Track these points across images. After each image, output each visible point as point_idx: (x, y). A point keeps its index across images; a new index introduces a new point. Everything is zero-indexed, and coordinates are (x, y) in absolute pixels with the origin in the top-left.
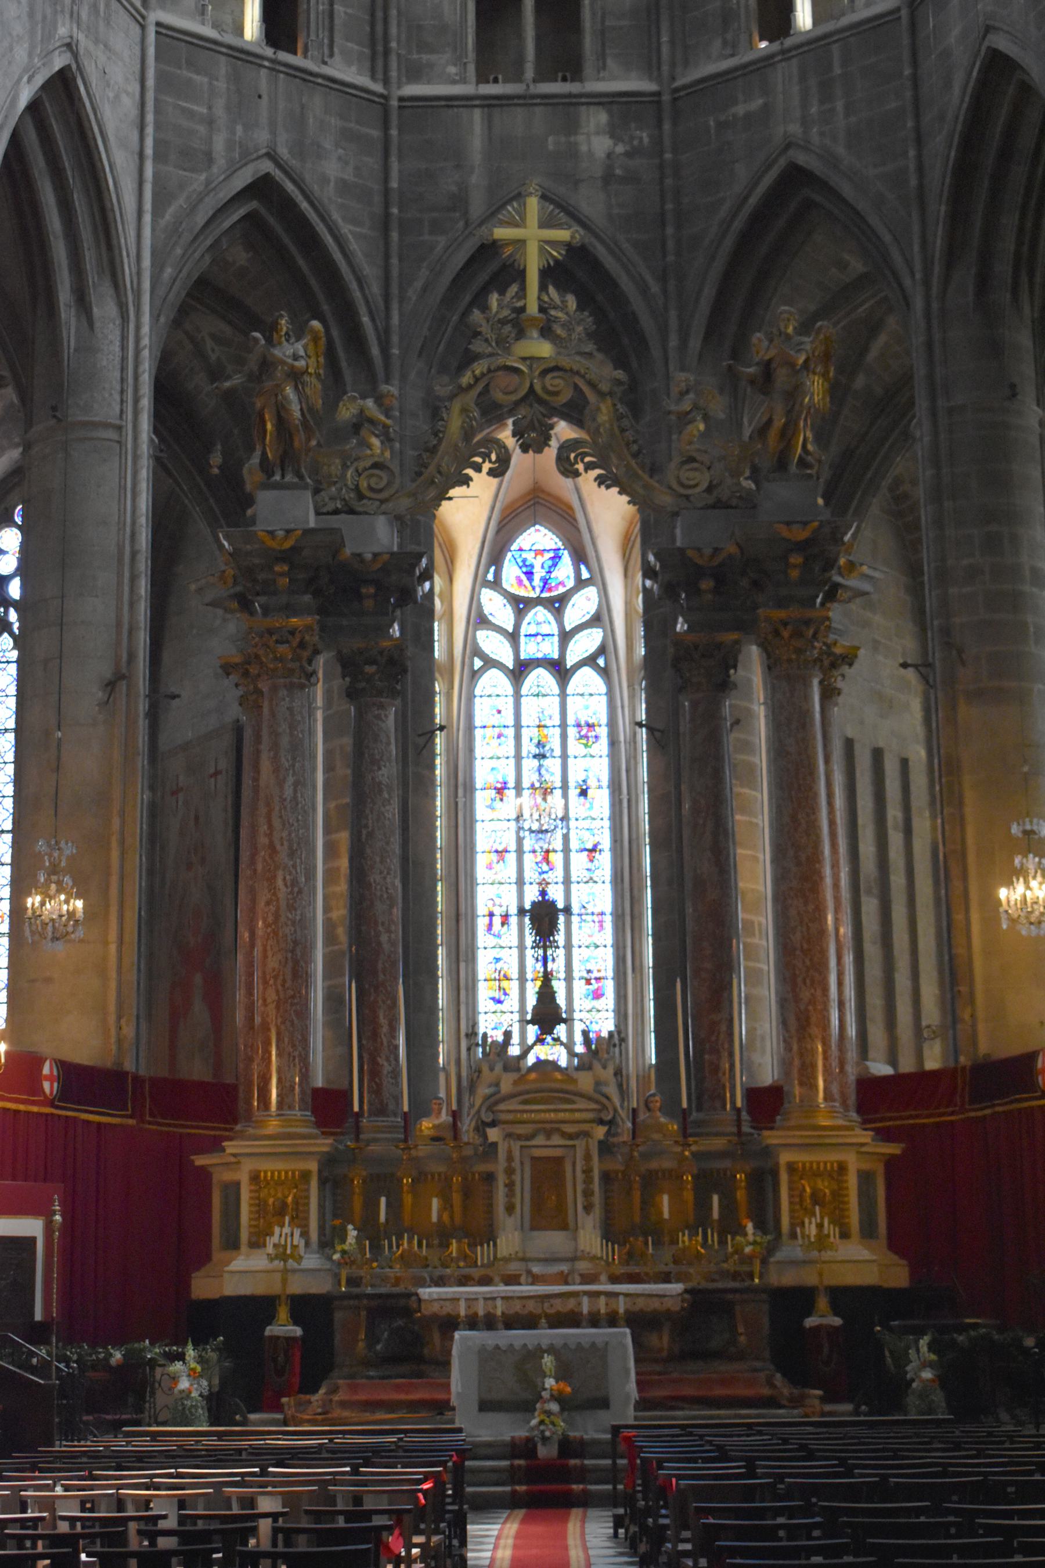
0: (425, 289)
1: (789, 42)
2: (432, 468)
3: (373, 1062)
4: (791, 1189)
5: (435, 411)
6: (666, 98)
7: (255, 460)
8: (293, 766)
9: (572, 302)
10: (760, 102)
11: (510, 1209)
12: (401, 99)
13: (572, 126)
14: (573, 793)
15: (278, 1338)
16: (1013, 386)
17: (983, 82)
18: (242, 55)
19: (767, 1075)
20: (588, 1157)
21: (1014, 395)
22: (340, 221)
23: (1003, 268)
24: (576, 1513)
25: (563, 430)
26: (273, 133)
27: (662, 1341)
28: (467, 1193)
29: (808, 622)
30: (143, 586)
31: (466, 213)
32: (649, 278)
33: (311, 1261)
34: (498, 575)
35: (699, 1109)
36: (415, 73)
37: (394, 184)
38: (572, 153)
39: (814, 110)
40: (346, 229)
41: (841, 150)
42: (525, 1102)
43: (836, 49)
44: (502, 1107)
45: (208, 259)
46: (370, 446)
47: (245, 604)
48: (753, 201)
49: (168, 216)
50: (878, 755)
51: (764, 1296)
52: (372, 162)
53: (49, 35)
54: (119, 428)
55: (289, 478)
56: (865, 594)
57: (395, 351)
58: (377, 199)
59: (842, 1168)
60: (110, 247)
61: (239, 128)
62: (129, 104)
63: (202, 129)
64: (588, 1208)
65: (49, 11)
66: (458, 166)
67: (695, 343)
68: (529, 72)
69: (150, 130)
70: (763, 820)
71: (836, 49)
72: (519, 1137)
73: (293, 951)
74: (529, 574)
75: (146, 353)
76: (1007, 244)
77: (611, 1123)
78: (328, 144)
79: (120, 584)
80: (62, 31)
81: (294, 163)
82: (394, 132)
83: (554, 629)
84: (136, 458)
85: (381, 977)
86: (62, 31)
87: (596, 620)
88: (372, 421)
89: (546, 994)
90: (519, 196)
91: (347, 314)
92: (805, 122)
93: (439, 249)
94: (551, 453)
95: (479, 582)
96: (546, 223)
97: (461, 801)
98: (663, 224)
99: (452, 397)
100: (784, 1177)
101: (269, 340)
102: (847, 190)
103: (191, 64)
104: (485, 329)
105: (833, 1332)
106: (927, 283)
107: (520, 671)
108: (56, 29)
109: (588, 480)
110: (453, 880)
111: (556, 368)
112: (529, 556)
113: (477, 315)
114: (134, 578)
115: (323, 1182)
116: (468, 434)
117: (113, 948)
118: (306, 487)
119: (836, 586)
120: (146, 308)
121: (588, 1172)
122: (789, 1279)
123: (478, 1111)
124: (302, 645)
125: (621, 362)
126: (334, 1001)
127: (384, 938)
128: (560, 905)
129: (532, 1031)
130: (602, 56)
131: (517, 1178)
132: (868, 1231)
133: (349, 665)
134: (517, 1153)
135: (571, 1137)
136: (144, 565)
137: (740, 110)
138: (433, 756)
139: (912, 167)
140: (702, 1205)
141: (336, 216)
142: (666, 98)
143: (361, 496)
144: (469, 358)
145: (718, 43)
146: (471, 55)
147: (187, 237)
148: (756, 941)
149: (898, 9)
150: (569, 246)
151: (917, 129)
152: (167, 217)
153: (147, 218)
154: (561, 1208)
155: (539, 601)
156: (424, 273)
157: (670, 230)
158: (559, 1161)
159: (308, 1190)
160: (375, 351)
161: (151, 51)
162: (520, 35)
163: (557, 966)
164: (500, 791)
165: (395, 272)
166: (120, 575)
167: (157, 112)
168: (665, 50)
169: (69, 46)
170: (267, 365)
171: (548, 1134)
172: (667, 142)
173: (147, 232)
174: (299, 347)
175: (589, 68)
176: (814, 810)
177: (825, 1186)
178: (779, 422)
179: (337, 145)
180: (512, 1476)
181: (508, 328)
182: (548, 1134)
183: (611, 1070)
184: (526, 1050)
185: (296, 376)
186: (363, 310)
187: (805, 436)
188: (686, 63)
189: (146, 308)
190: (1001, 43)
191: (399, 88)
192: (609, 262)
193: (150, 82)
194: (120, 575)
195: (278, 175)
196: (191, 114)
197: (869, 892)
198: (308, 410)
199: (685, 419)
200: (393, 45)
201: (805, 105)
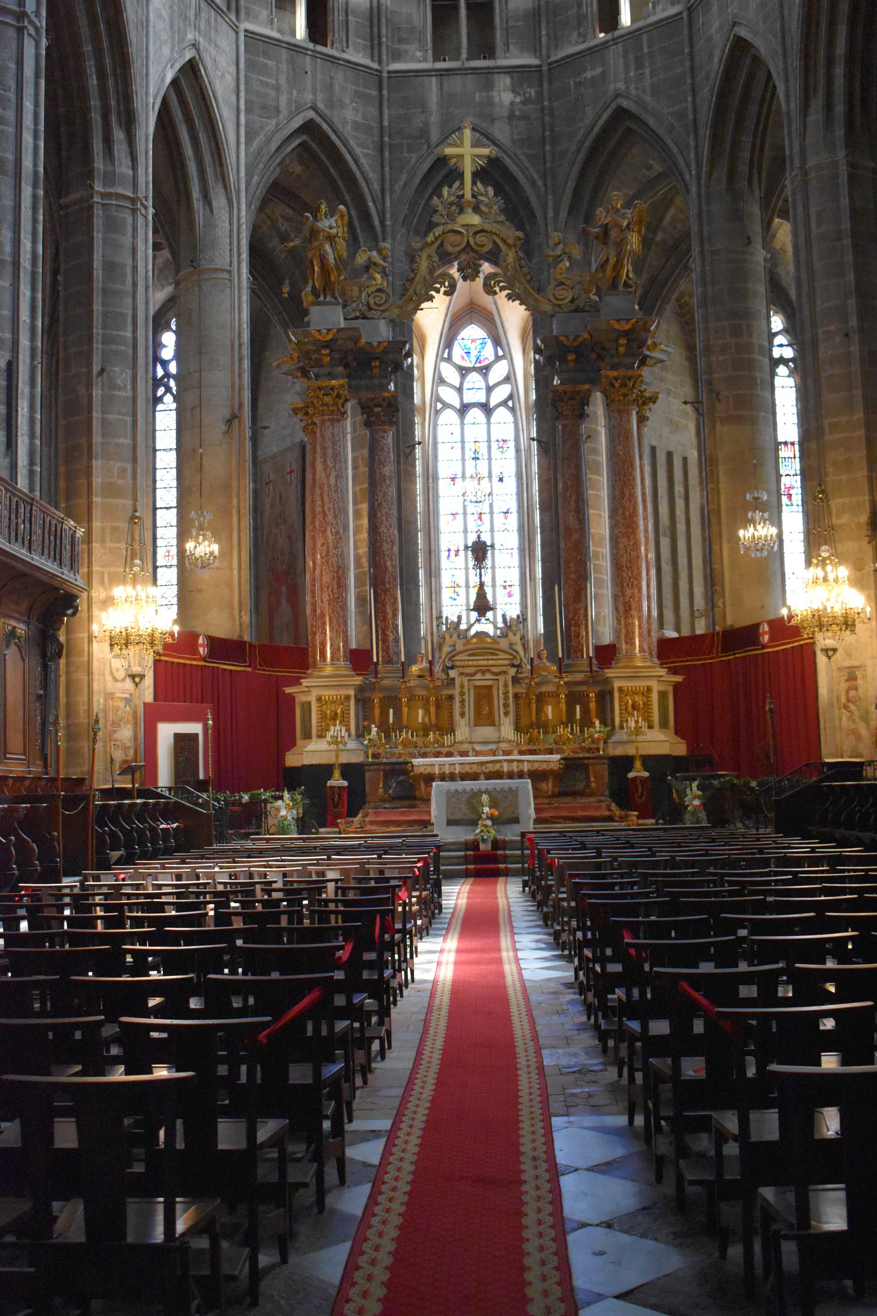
0: (405, 185)
1: (617, 33)
2: (411, 291)
3: (384, 633)
4: (620, 701)
5: (412, 260)
6: (545, 68)
8: (334, 466)
9: (491, 191)
10: (600, 70)
12: (389, 72)
13: (489, 86)
14: (495, 479)
15: (334, 787)
16: (749, 238)
17: (731, 56)
18: (295, 48)
19: (607, 639)
20: (506, 686)
21: (750, 243)
22: (355, 146)
23: (743, 168)
24: (501, 879)
25: (487, 268)
26: (314, 94)
27: (548, 786)
28: (438, 707)
29: (630, 379)
31: (428, 141)
32: (535, 176)
33: (352, 745)
34: (450, 354)
35: (569, 658)
36: (397, 56)
37: (386, 123)
38: (490, 102)
39: (632, 74)
40: (358, 151)
41: (648, 98)
42: (470, 655)
43: (645, 38)
44: (457, 658)
45: (278, 169)
46: (375, 279)
47: (305, 374)
48: (596, 129)
50: (670, 455)
51: (606, 761)
52: (373, 111)
53: (182, 40)
54: (230, 272)
55: (328, 299)
56: (663, 361)
57: (388, 223)
58: (376, 132)
59: (649, 689)
60: (221, 165)
61: (295, 92)
62: (230, 80)
63: (273, 93)
64: (506, 714)
65: (182, 25)
66: (423, 112)
67: (563, 215)
68: (464, 55)
69: (242, 94)
70: (604, 493)
71: (645, 38)
72: (467, 675)
73: (337, 572)
75: (244, 227)
76: (745, 154)
77: (519, 666)
78: (347, 102)
79: (233, 363)
80: (190, 36)
81: (326, 111)
82: (385, 92)
83: (483, 385)
84: (240, 288)
85: (388, 586)
86: (190, 36)
87: (507, 379)
88: (375, 264)
89: (481, 594)
91: (359, 202)
92: (627, 81)
93: (413, 162)
94: (480, 281)
95: (439, 358)
96: (475, 144)
97: (431, 485)
98: (544, 145)
99: (422, 249)
100: (616, 695)
101: (315, 217)
102: (651, 122)
103: (266, 54)
104: (440, 208)
105: (643, 780)
106: (699, 179)
107: (464, 409)
108: (186, 35)
109: (502, 297)
110: (427, 530)
111: (482, 231)
112: (468, 343)
113: (435, 200)
114: (241, 360)
115: (357, 701)
116: (431, 271)
117: (236, 572)
118: (338, 304)
119: (646, 357)
120: (243, 200)
121: (506, 694)
122: (619, 751)
123: (444, 661)
124: (339, 396)
125: (520, 227)
126: (361, 600)
127: (389, 564)
128: (489, 543)
129: (474, 615)
130: (507, 44)
131: (466, 697)
132: (664, 724)
133: (365, 408)
134: (466, 684)
135: (496, 674)
136: (246, 351)
137: (589, 74)
138: (415, 459)
139: (690, 106)
140: (571, 711)
141: (352, 143)
142: (545, 68)
143: (370, 309)
144: (432, 226)
146: (430, 44)
147: (265, 159)
148: (600, 562)
149: (681, 13)
150: (489, 157)
151: (693, 84)
152: (254, 146)
154: (491, 713)
155: (474, 369)
156: (404, 176)
157: (548, 148)
158: (490, 687)
159: (349, 706)
160: (377, 223)
161: (242, 47)
163: (487, 579)
164: (453, 479)
165: (387, 176)
166: (233, 357)
167: (247, 83)
168: (544, 40)
169: (194, 45)
170: (314, 233)
171: (483, 673)
172: (546, 95)
174: (332, 221)
176: (633, 487)
177: (639, 700)
178: (613, 261)
179: (352, 101)
180: (466, 860)
181: (454, 208)
182: (483, 673)
183: (518, 637)
184: (470, 627)
185: (331, 239)
186: (369, 198)
187: (627, 269)
188: (556, 47)
189: (243, 200)
190: (743, 33)
191: (388, 65)
192: (512, 167)
193: (242, 65)
194: (233, 357)
195: (318, 119)
196: (267, 84)
197: (664, 534)
198: (339, 259)
199: (558, 259)
200: (384, 39)
201: (627, 71)
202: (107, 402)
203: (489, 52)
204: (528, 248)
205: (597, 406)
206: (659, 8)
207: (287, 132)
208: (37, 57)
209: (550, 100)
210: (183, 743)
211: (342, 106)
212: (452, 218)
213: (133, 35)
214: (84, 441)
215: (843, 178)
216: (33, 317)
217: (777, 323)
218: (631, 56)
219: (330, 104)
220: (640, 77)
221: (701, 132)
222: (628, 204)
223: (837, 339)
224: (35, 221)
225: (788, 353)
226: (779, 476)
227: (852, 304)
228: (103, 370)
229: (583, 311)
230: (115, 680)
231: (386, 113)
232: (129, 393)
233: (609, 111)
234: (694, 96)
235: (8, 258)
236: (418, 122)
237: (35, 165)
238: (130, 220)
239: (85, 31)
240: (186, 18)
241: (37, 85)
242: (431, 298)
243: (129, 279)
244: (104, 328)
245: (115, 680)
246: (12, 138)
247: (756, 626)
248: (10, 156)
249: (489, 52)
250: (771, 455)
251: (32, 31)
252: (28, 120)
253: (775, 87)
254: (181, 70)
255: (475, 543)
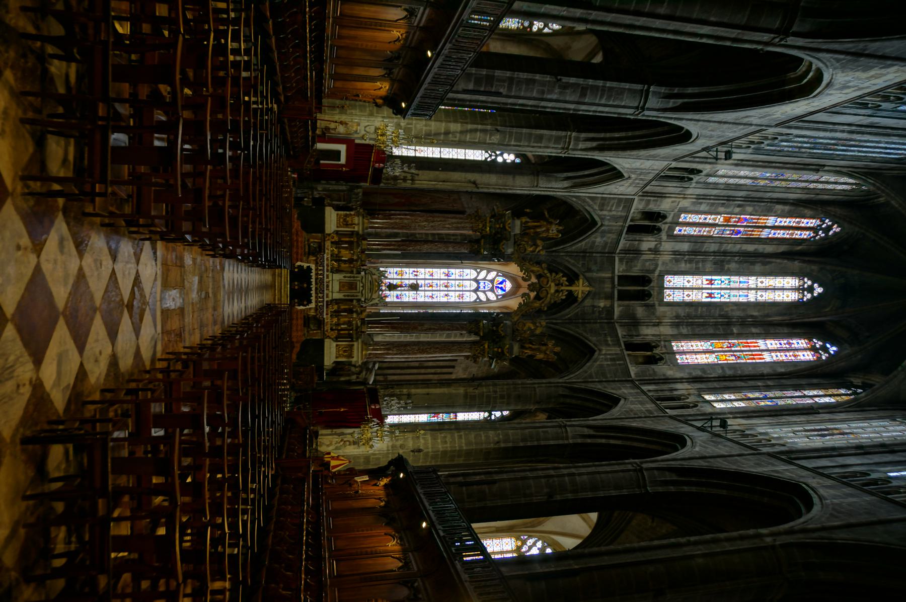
5: (539, 263)
7: (528, 220)
11: (345, 277)
14: (446, 293)
23: (568, 401)
25: (533, 295)
26: (608, 226)
27: (312, 313)
30: (498, 191)
34: (500, 276)
36: (621, 260)
37: (594, 255)
38: (599, 299)
39: (608, 357)
40: (584, 243)
41: (598, 363)
48: (587, 341)
49: (588, 200)
52: (599, 250)
53: (632, 173)
54: (537, 186)
57: (554, 254)
58: (591, 250)
62: (615, 191)
63: (609, 208)
64: (344, 296)
68: (620, 288)
69: (609, 196)
74: (501, 283)
75: (555, 193)
76: (574, 401)
78: (604, 239)
80: (633, 176)
81: (600, 230)
90: (590, 285)
94: (527, 291)
102: (588, 364)
103: (624, 207)
111: (548, 293)
116: (533, 271)
124: (483, 230)
136: (504, 191)
137: (609, 339)
143: (518, 245)
144: (551, 271)
145: (625, 334)
150: (577, 297)
153: (587, 195)
156: (573, 261)
160: (554, 249)
162: (629, 286)
167: (614, 198)
170: (551, 223)
171: (363, 287)
173: (584, 195)
175: (620, 302)
176: (439, 353)
181: (557, 282)
182: (363, 287)
188: (621, 326)
190: (622, 402)
196: (612, 206)
199: (534, 324)
201: (609, 354)
202: (484, 131)
203: (619, 299)
204: (539, 311)
205: (473, 338)
206: (634, 368)
207: (593, 214)
208: (627, 114)
209: (600, 323)
210: (336, 155)
211: (602, 237)
212: (553, 281)
213: (634, 153)
214: (469, 120)
215: (561, 442)
216: (520, 105)
217: (506, 413)
218: (614, 356)
219: (604, 232)
220: (606, 360)
221: (583, 384)
222: (555, 353)
223: (496, 439)
224: (560, 109)
225: (493, 417)
226: (443, 413)
227: (510, 445)
228: (498, 131)
229: (513, 334)
230: (365, 127)
231: (598, 255)
232: (488, 141)
233: (593, 347)
234: (599, 382)
235: (545, 96)
236: (594, 268)
237: (583, 110)
238: (560, 146)
239: (637, 133)
240: (641, 174)
241: (615, 113)
242: (521, 271)
243: (536, 145)
244: (516, 133)
245: (365, 127)
246: (593, 101)
247: (378, 403)
248: (586, 100)
249: (619, 299)
250: (451, 410)
251: (637, 113)
252: (600, 109)
253: (599, 414)
254: (620, 172)
255: (417, 284)
